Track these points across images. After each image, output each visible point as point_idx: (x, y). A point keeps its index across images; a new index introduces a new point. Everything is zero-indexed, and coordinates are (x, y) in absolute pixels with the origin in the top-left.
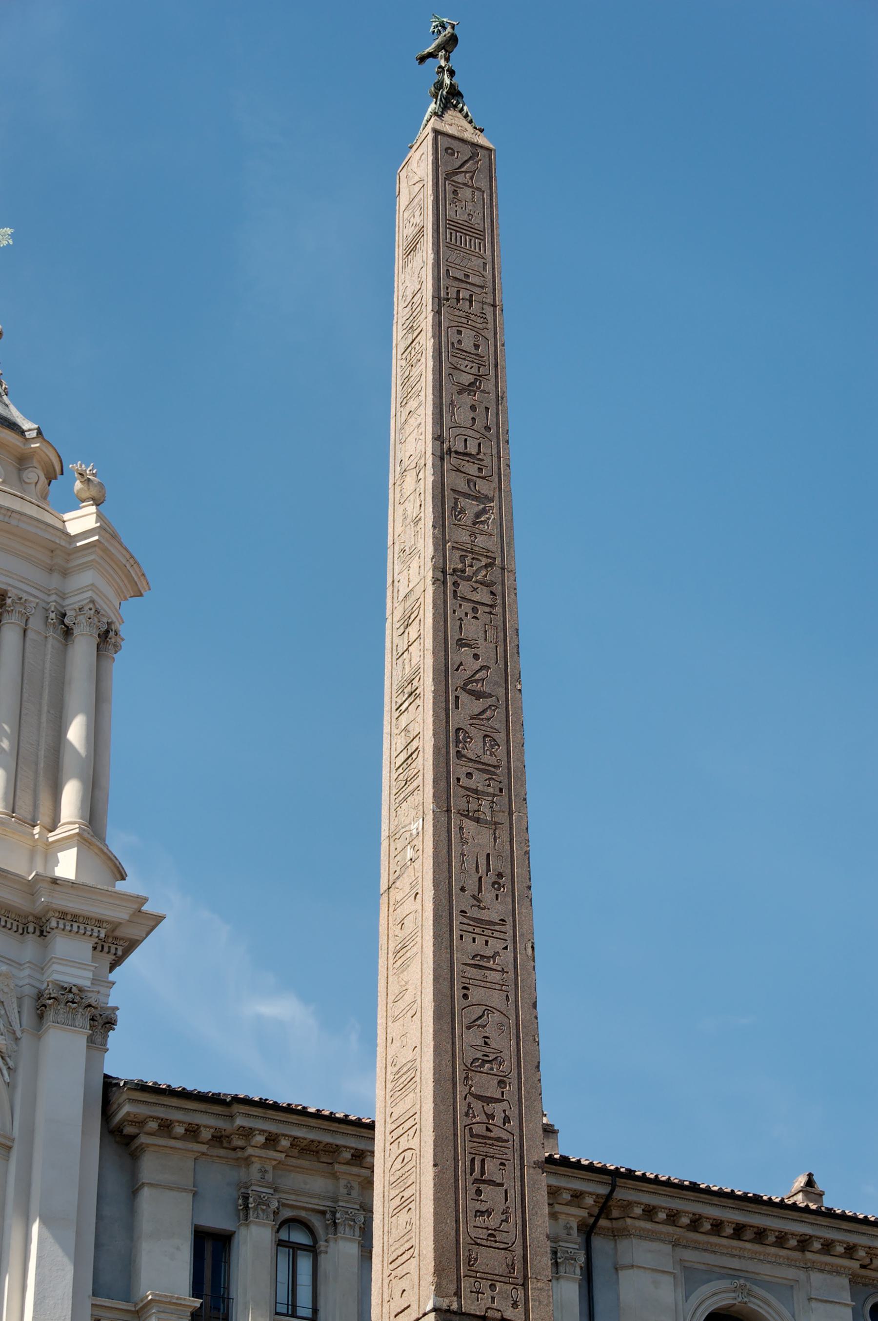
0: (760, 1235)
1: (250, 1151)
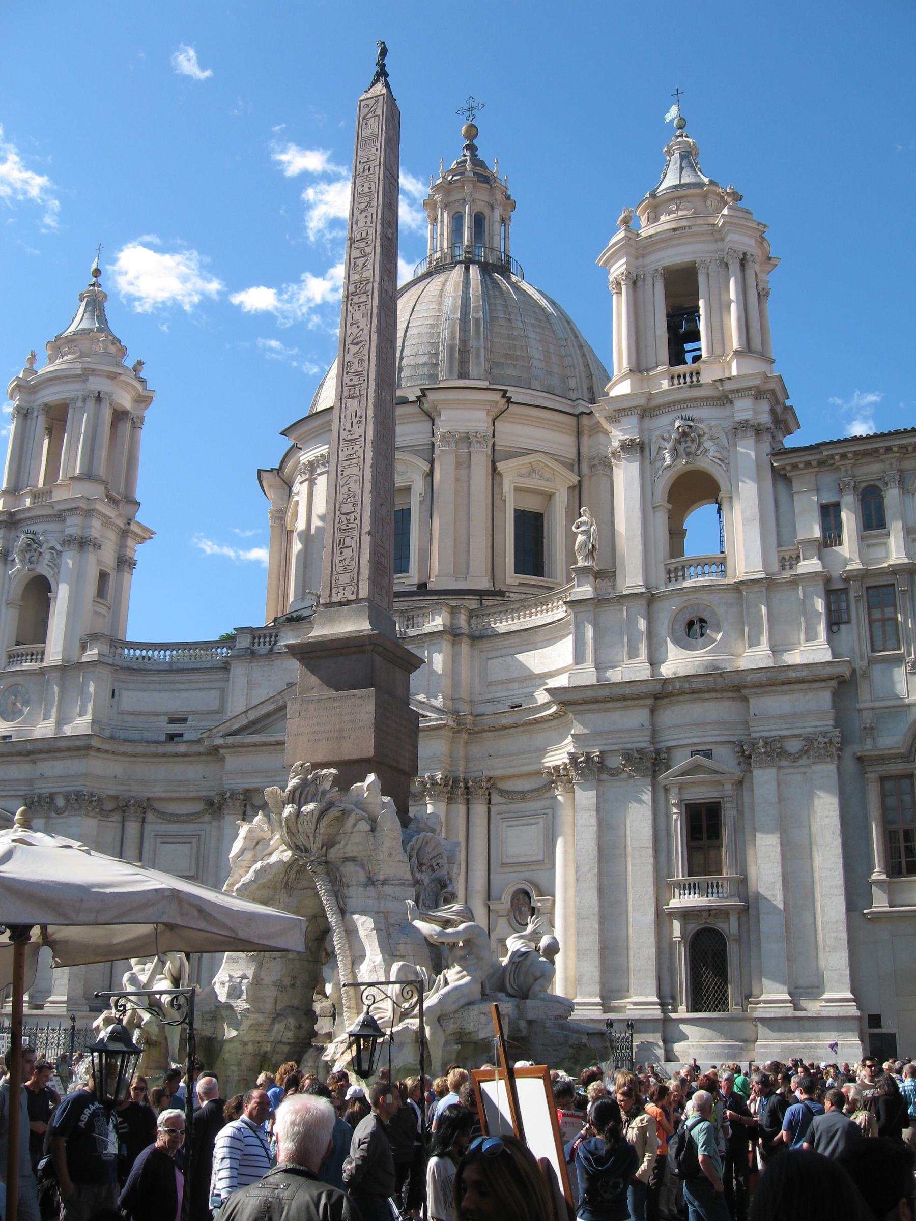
1: (837, 464)
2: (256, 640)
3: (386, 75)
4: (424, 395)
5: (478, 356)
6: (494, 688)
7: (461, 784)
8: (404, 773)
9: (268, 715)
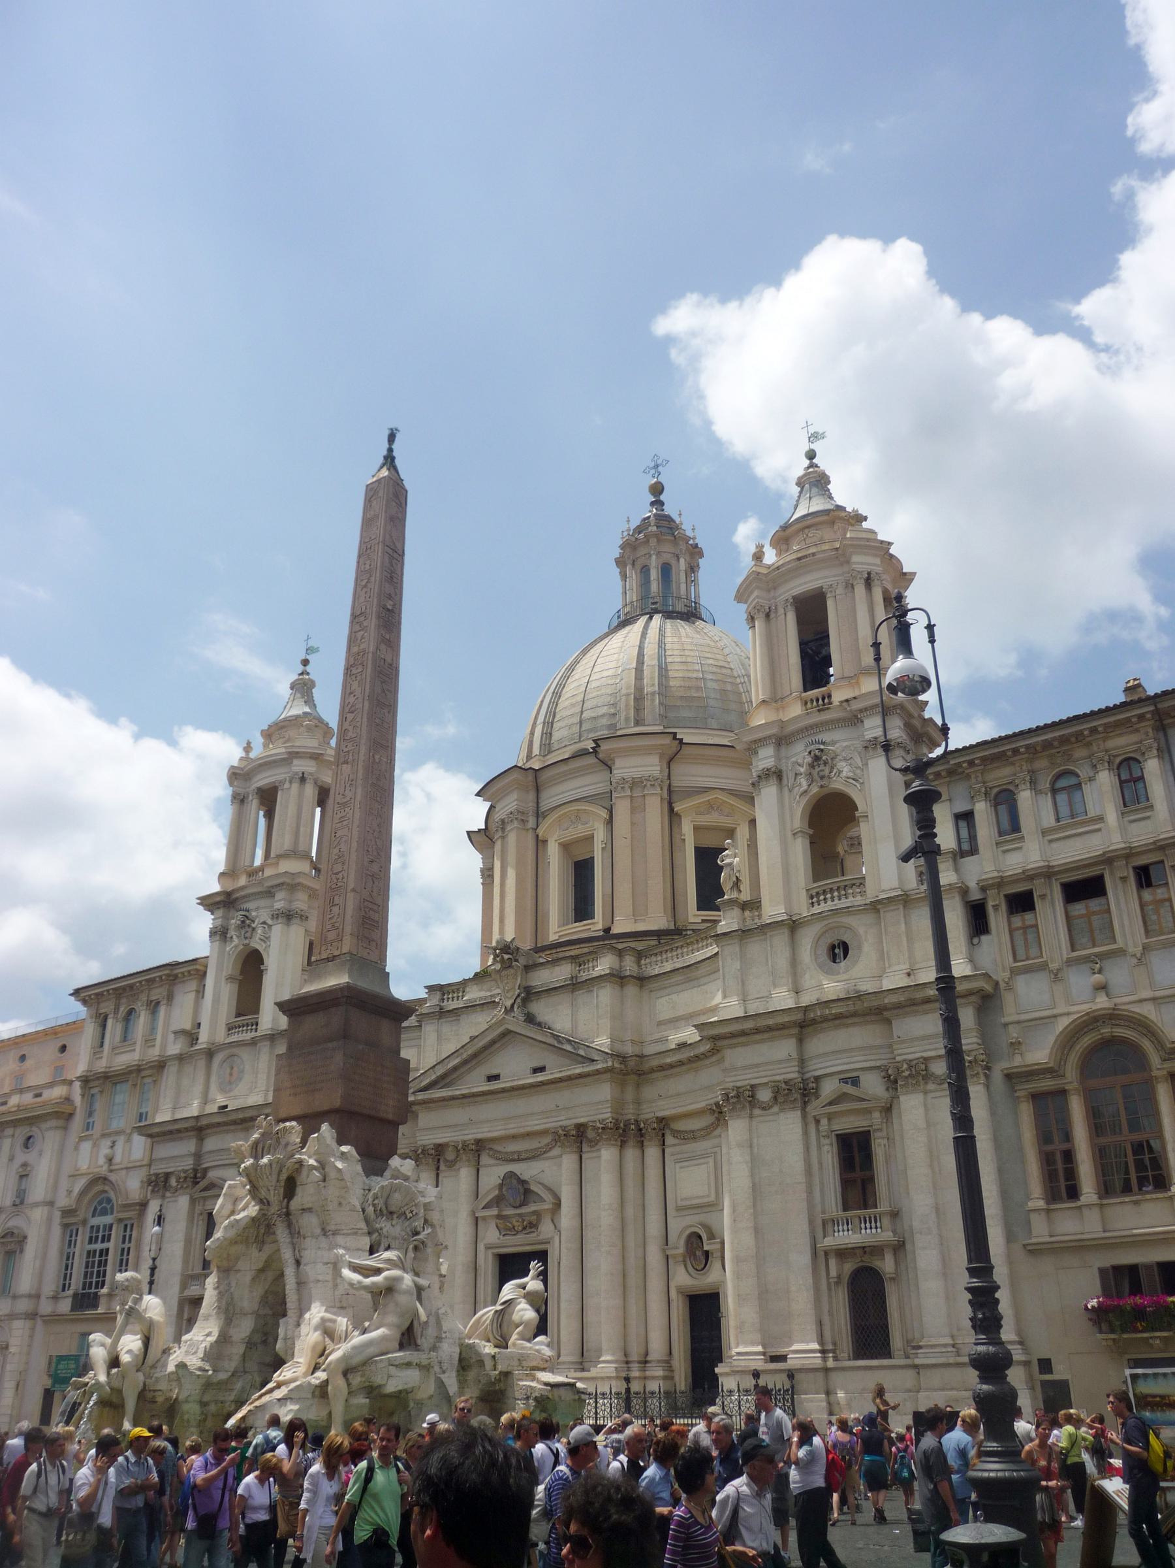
2: (446, 997)
3: (393, 459)
4: (598, 746)
5: (653, 700)
6: (663, 1027)
7: (633, 1127)
8: (389, 1122)
9: (455, 1069)
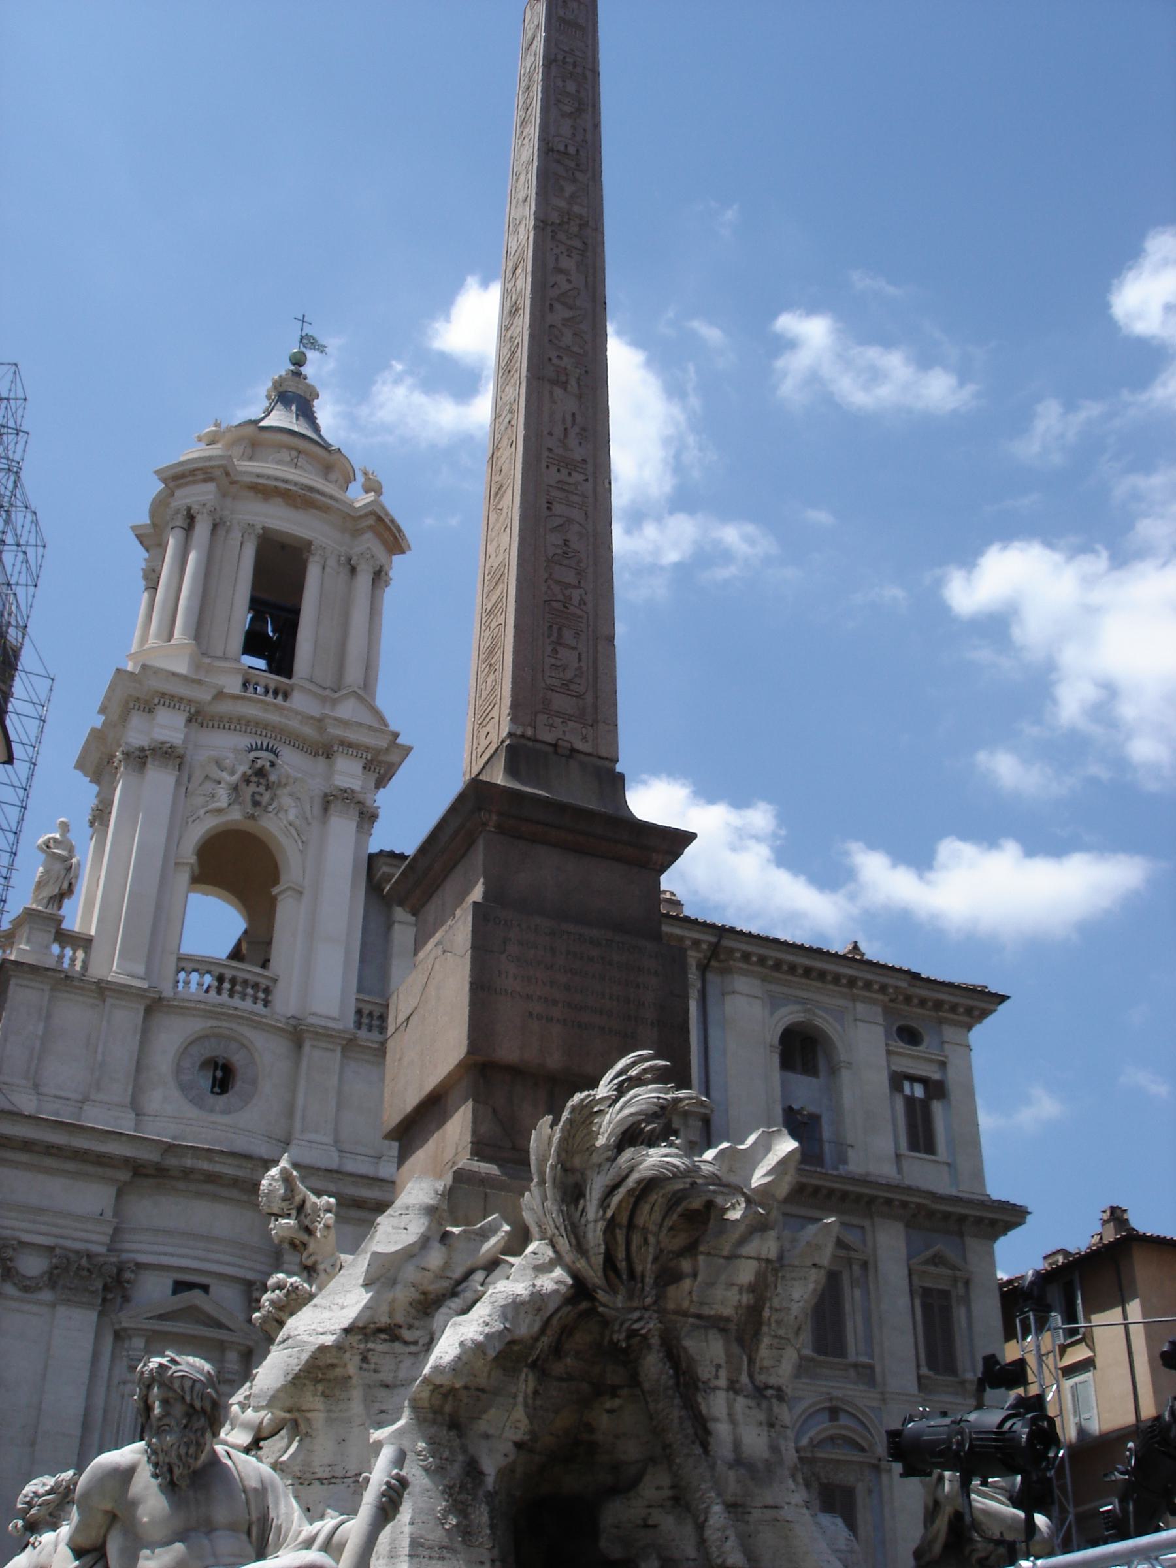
0: (822, 975)
